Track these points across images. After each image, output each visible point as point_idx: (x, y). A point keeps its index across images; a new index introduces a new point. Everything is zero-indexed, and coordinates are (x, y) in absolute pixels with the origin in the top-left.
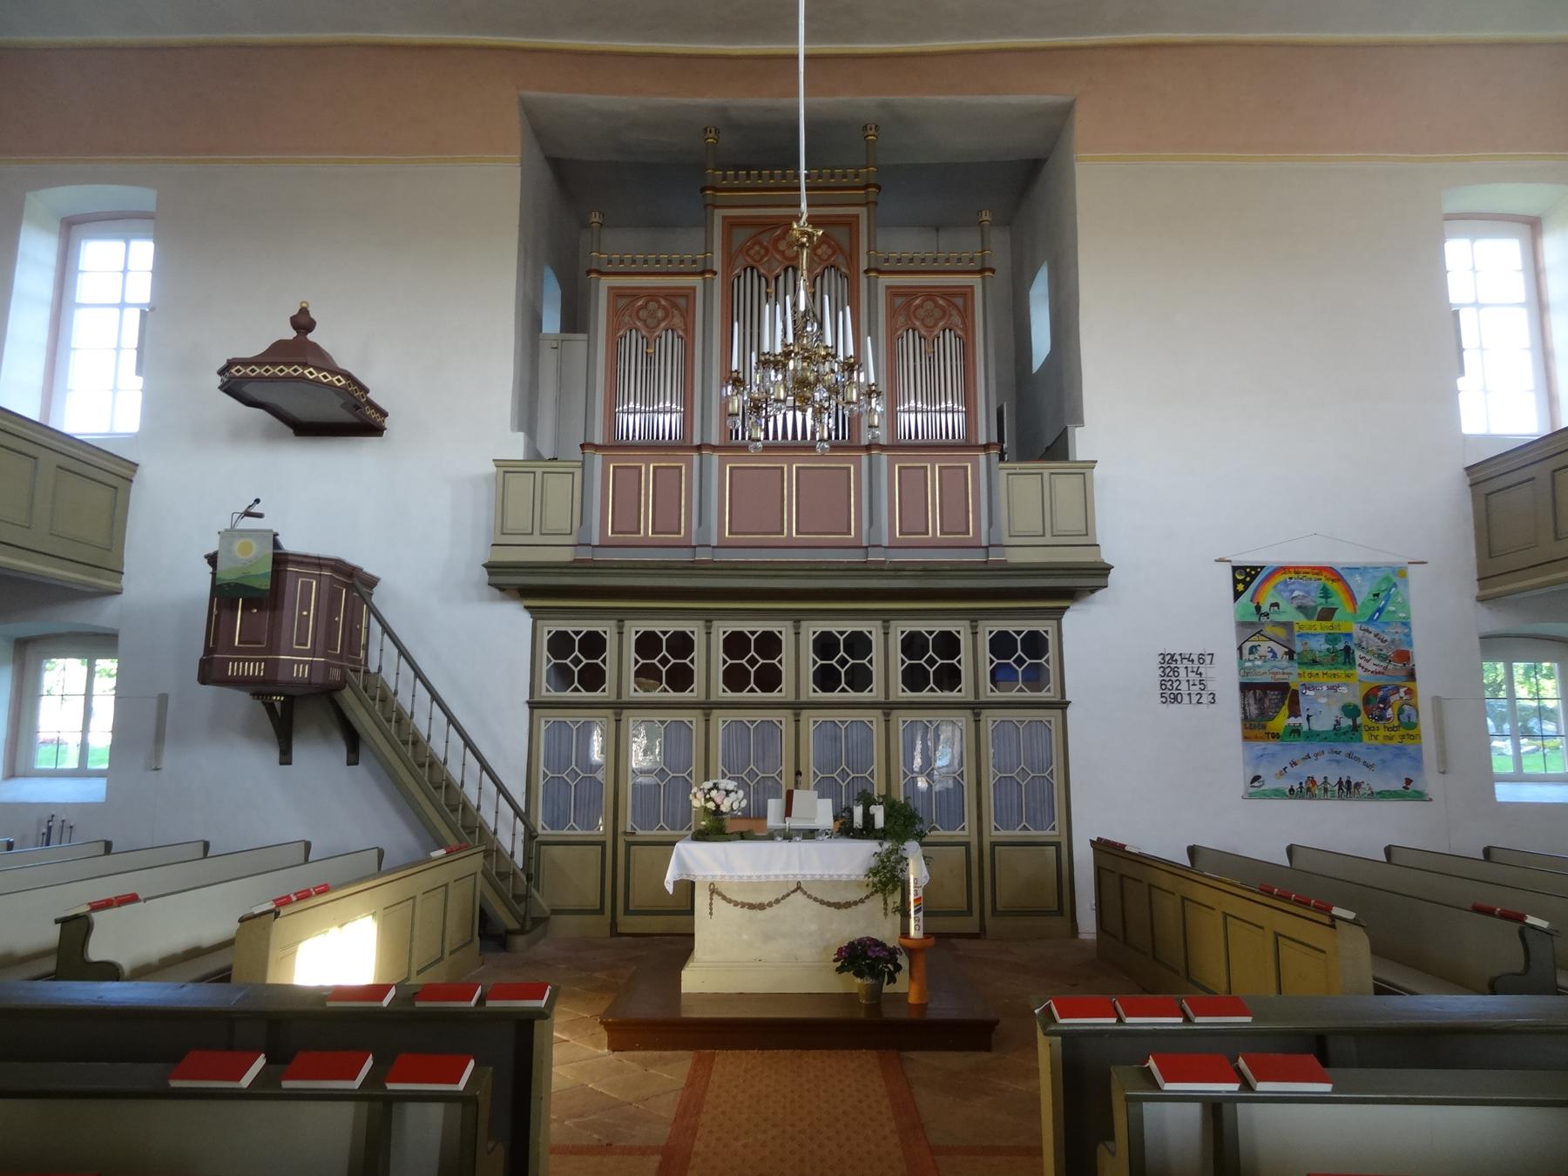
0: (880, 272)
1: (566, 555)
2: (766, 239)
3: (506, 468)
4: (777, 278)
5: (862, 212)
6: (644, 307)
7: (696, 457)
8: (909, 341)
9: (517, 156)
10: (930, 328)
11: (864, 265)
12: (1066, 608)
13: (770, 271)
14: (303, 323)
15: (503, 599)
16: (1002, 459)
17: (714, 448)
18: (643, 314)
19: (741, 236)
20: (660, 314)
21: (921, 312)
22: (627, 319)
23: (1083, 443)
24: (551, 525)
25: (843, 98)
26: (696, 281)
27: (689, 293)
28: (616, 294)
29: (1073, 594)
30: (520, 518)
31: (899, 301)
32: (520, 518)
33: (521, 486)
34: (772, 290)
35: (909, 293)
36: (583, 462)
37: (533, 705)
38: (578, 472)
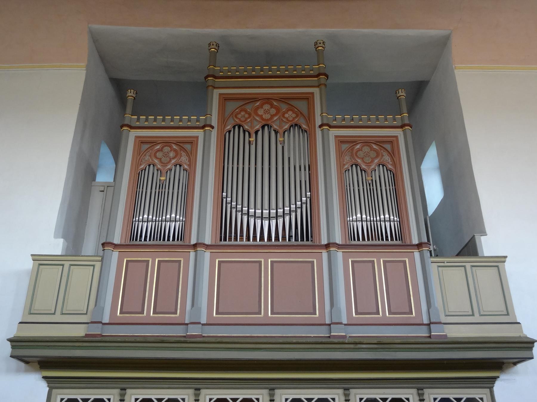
0: (331, 127)
1: (79, 332)
2: (249, 108)
4: (256, 132)
5: (316, 91)
6: (161, 150)
7: (192, 254)
8: (354, 175)
9: (84, 64)
10: (368, 164)
11: (318, 122)
12: (495, 378)
13: (252, 127)
15: (26, 371)
16: (431, 255)
17: (207, 247)
18: (159, 155)
19: (231, 106)
20: (172, 154)
21: (361, 154)
22: (147, 157)
23: (488, 246)
24: (71, 306)
25: (300, 30)
26: (199, 133)
27: (193, 142)
28: (141, 141)
29: (499, 366)
30: (46, 301)
31: (345, 146)
32: (46, 301)
33: (52, 274)
34: (253, 139)
35: (352, 141)
36: (103, 258)
38: (98, 265)
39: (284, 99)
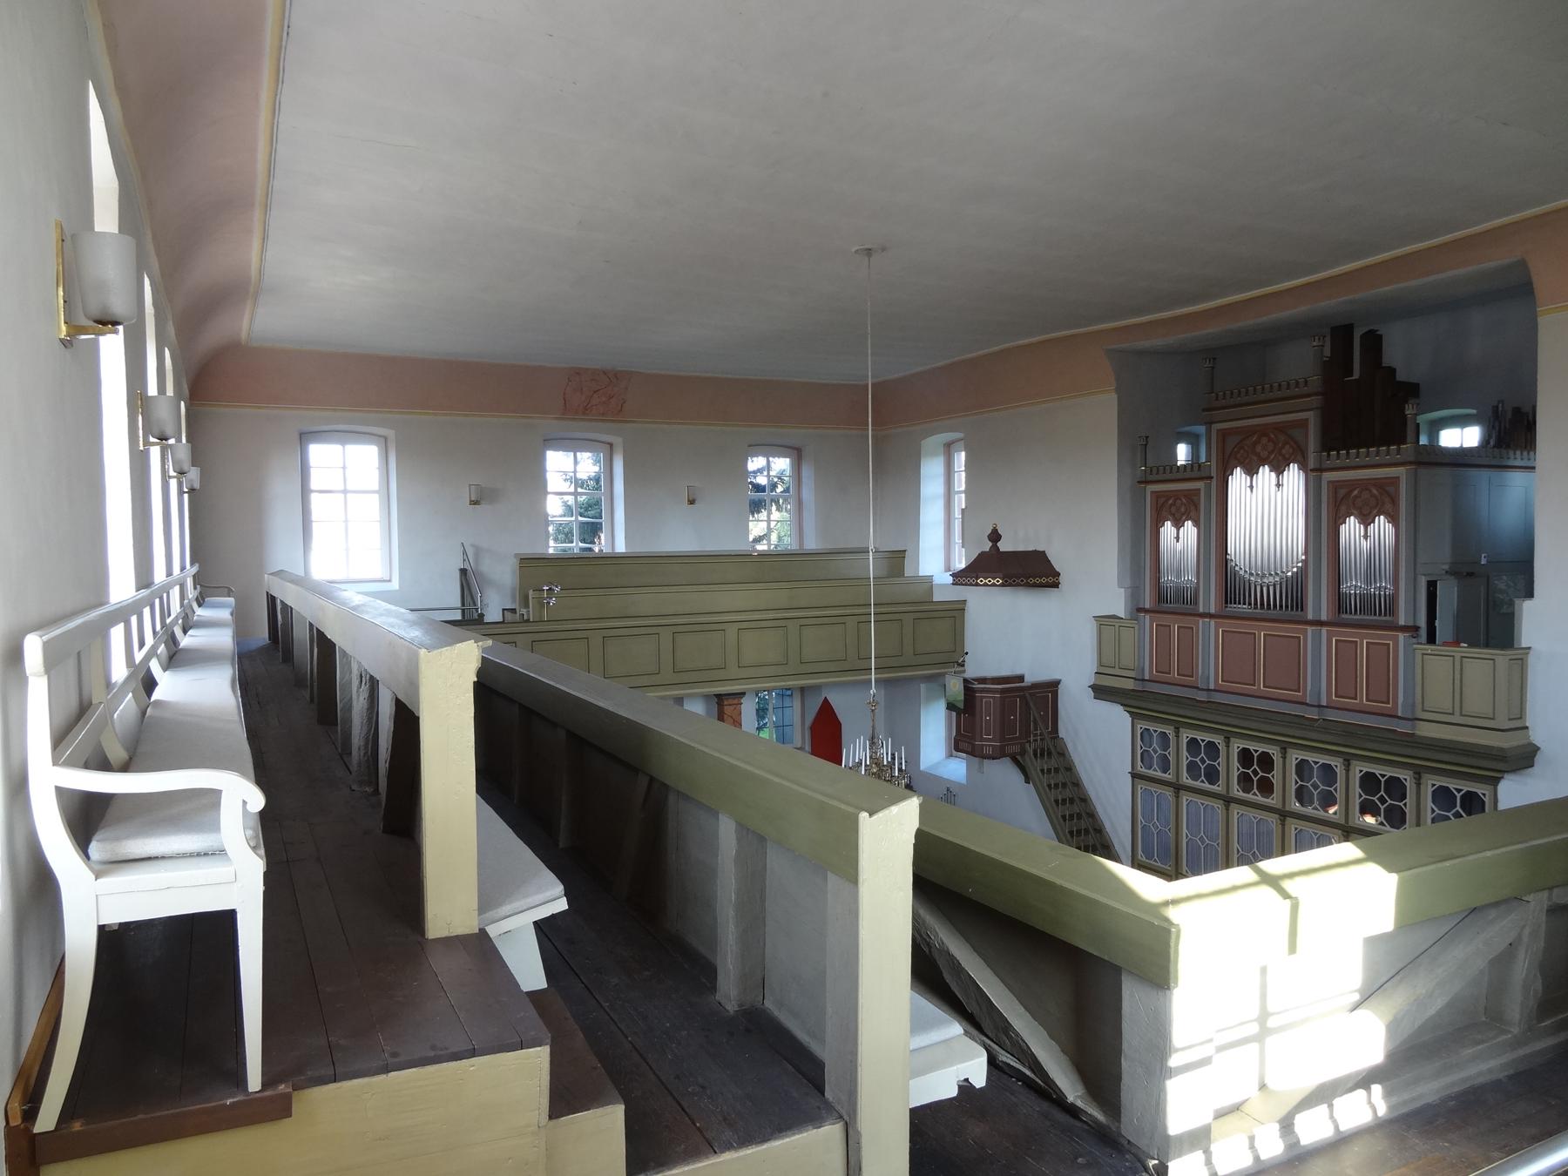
1: (1129, 685)
3: (1104, 621)
14: (995, 537)
17: (1211, 616)
26: (1200, 485)
37: (1135, 776)
39: (1280, 428)
